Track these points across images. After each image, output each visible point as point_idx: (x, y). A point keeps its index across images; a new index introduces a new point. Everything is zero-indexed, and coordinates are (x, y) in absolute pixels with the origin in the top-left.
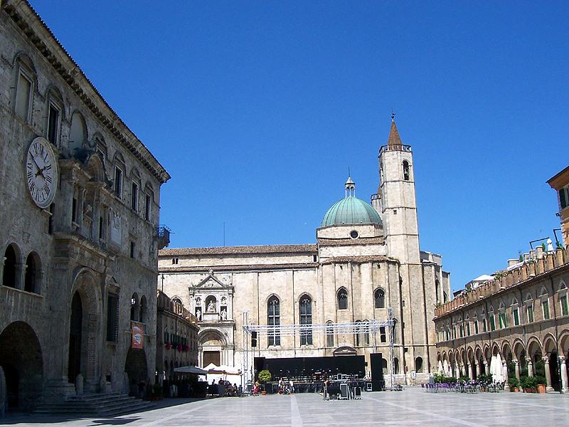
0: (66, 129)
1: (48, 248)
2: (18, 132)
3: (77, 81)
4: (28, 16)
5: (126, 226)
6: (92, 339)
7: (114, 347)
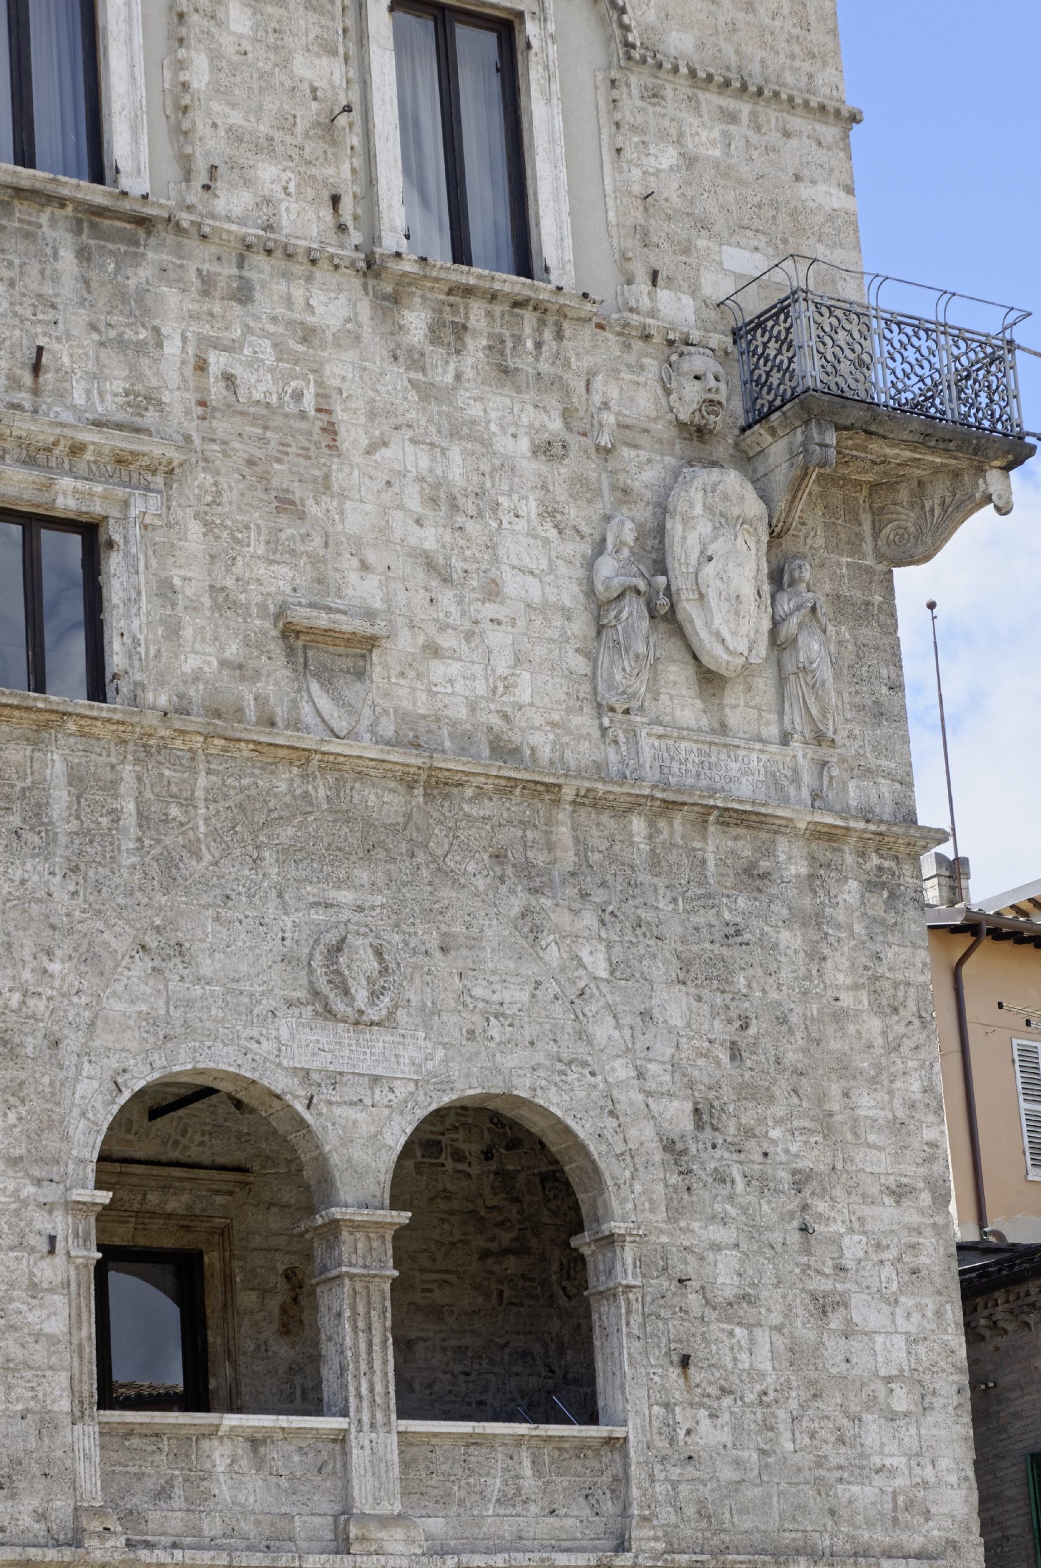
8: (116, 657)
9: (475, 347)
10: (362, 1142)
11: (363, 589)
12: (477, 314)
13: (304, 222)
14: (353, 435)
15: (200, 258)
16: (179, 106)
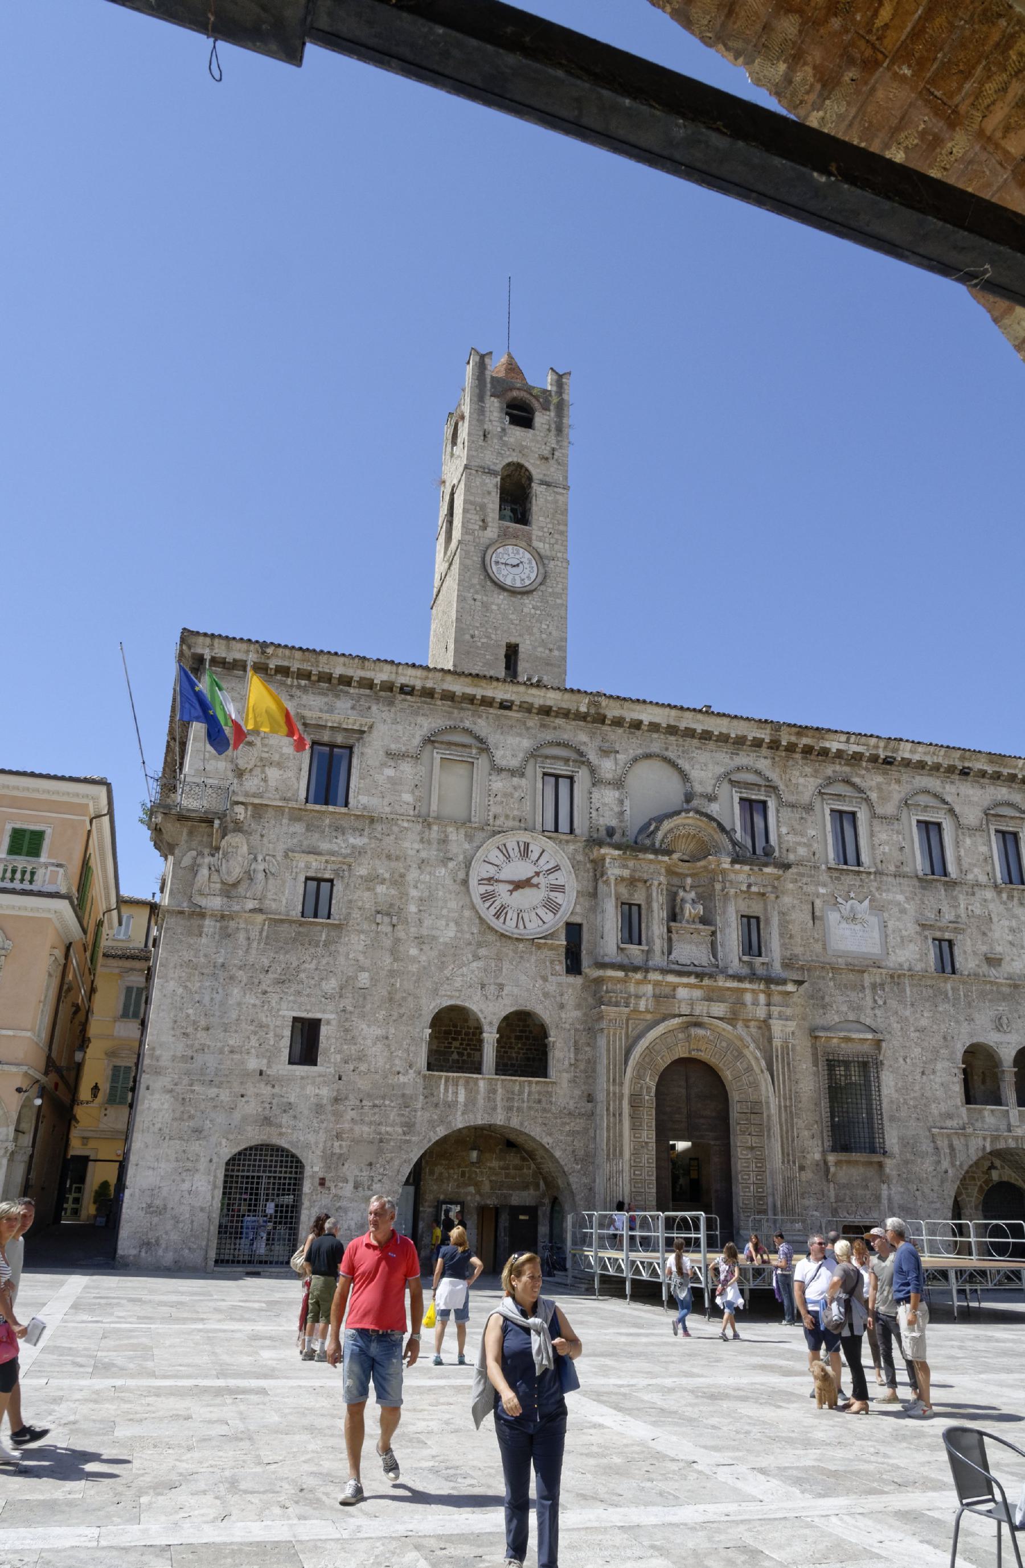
0: (609, 796)
1: (570, 998)
2: (444, 841)
3: (613, 711)
4: (427, 678)
5: (903, 911)
6: (752, 1148)
7: (880, 1165)
8: (957, 965)
9: (1016, 899)
10: (1007, 1055)
11: (999, 949)
12: (1015, 893)
13: (983, 879)
14: (995, 919)
15: (965, 888)
16: (959, 859)
